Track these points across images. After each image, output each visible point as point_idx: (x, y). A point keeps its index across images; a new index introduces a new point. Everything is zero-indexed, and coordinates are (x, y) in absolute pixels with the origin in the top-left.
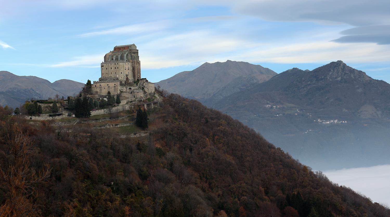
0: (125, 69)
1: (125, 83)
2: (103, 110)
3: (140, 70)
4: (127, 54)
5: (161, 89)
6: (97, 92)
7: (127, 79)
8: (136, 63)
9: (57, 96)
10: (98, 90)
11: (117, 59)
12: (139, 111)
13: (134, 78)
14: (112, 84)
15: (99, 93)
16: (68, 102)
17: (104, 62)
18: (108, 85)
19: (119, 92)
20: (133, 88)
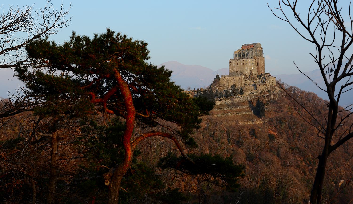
0: (249, 65)
1: (249, 77)
2: (227, 101)
3: (264, 65)
4: (252, 51)
5: (281, 83)
6: (224, 85)
7: (251, 73)
8: (260, 60)
9: (189, 88)
10: (225, 83)
11: (243, 55)
12: (258, 102)
13: (259, 73)
14: (237, 78)
15: (226, 86)
16: (198, 93)
17: (233, 58)
18: (234, 79)
19: (243, 85)
20: (255, 81)
